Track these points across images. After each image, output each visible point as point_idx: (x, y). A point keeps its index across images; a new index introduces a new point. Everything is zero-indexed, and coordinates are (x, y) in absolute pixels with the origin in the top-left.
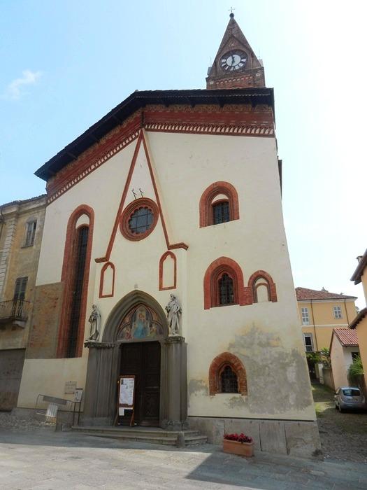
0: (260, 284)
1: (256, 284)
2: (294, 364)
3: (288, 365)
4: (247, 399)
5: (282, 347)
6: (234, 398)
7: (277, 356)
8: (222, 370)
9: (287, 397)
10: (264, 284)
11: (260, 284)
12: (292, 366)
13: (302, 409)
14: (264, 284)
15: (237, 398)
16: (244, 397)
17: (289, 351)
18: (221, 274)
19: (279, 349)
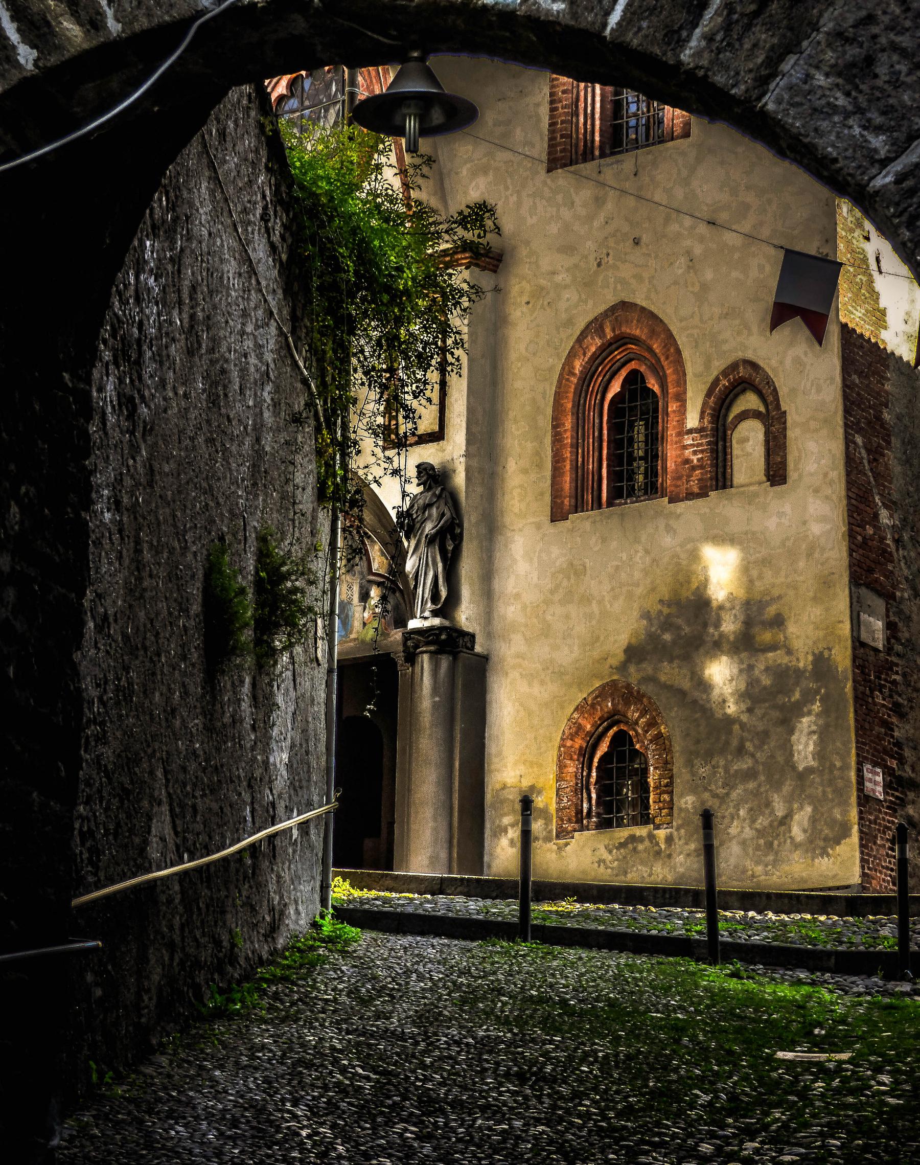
0: (744, 416)
1: (736, 410)
2: (817, 707)
3: (797, 710)
4: (669, 839)
5: (789, 652)
6: (633, 839)
7: (766, 681)
8: (603, 748)
9: (785, 821)
10: (757, 415)
11: (744, 416)
12: (809, 713)
13: (824, 853)
14: (757, 415)
15: (641, 840)
16: (661, 833)
17: (804, 662)
18: (623, 373)
19: (776, 657)
